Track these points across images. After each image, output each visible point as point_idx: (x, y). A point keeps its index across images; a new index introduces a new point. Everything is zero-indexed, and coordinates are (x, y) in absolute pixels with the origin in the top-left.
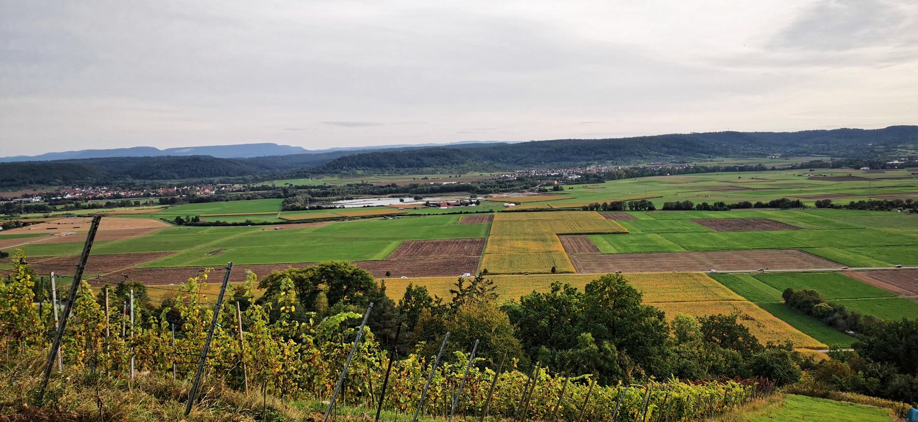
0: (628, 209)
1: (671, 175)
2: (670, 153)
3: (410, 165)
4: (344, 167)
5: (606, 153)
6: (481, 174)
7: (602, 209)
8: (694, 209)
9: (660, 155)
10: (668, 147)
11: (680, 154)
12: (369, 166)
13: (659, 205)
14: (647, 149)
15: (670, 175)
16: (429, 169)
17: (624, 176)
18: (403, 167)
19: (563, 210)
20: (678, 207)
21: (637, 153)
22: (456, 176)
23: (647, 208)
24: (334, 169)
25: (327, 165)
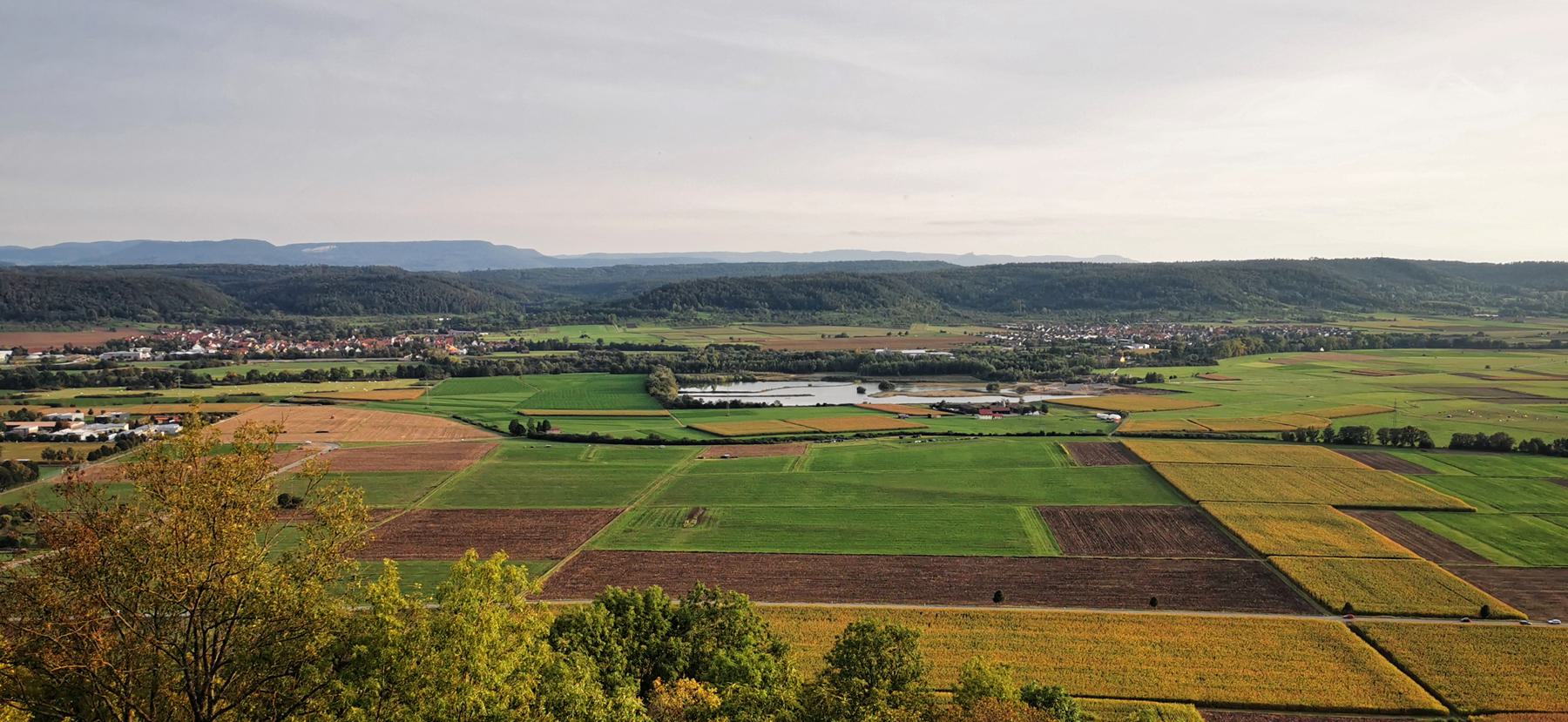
0: (1377, 442)
1: (1326, 350)
2: (1286, 300)
3: (797, 306)
4: (675, 305)
5: (1165, 295)
6: (943, 329)
7: (1322, 441)
8: (1515, 451)
9: (1267, 302)
10: (1279, 288)
11: (1305, 302)
12: (718, 302)
13: (1442, 440)
14: (1241, 290)
15: (1325, 350)
16: (834, 315)
17: (1242, 351)
18: (784, 308)
19: (1227, 438)
20: (1482, 445)
21: (1226, 299)
22: (900, 334)
23: (1417, 444)
24: (657, 307)
25: (644, 299)
